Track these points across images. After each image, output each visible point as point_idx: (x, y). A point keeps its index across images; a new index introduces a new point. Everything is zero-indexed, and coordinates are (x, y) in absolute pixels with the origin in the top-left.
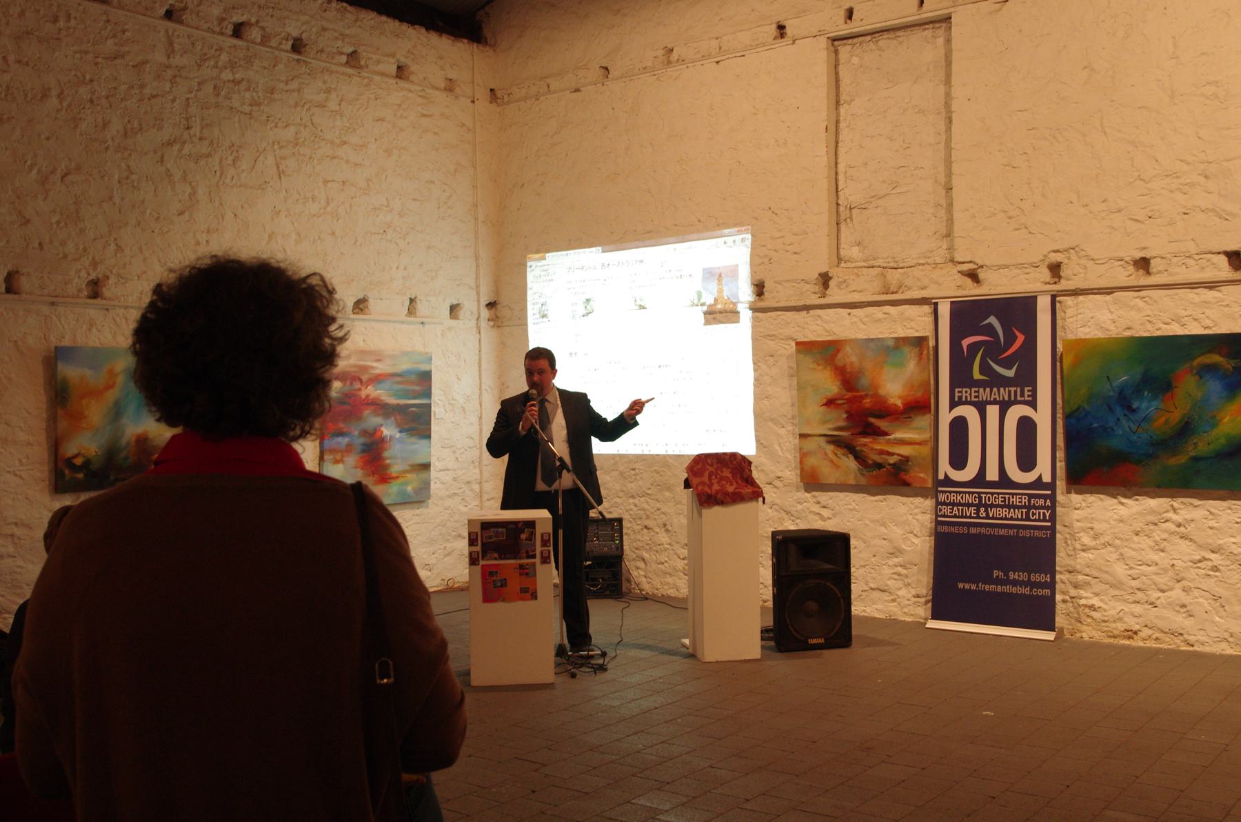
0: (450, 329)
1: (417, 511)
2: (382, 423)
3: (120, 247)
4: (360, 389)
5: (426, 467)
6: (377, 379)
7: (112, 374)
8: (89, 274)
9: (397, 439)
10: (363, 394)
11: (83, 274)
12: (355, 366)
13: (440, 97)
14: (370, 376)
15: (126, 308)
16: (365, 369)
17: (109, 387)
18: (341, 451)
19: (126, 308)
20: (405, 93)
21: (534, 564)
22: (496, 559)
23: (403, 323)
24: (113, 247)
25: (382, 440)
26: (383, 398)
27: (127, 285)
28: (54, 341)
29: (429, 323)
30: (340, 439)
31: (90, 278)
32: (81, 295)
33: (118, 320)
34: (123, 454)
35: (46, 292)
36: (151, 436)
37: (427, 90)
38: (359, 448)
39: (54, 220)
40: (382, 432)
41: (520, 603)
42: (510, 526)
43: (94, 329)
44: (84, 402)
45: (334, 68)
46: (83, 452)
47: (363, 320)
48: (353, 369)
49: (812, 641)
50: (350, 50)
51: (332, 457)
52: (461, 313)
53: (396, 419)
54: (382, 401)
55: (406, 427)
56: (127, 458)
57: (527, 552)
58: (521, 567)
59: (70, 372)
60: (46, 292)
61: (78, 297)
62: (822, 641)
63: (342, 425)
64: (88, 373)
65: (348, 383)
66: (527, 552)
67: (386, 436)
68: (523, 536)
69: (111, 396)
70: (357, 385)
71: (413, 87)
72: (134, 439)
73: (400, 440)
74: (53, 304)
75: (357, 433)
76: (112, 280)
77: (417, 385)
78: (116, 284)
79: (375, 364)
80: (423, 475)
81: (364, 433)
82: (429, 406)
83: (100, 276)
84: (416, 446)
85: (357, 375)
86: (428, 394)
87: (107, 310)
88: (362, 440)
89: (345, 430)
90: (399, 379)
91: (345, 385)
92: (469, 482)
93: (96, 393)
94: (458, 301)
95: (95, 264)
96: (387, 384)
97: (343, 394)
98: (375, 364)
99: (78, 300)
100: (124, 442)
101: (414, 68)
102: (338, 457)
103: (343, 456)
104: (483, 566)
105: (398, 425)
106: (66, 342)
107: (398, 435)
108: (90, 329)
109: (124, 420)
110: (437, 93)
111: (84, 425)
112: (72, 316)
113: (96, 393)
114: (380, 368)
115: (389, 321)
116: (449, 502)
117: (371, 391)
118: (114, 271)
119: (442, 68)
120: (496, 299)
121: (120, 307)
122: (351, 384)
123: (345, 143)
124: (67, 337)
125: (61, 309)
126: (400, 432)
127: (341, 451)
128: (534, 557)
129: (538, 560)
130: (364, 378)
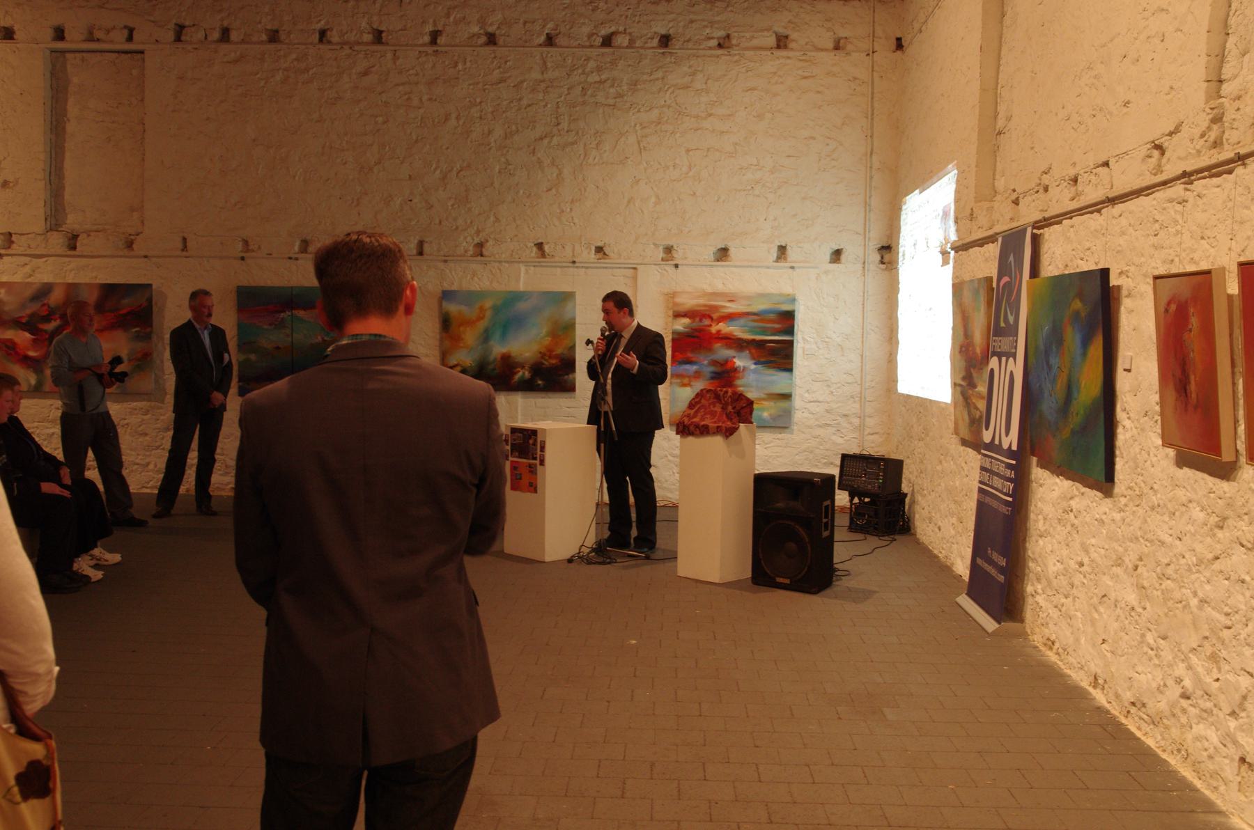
0: (826, 272)
1: (780, 436)
2: (735, 355)
3: (498, 219)
4: (711, 325)
5: (787, 397)
6: (730, 317)
7: (482, 309)
8: (473, 240)
9: (752, 370)
10: (714, 329)
11: (469, 239)
12: (705, 306)
13: (829, 58)
14: (722, 314)
15: (500, 262)
16: (716, 308)
17: (480, 318)
18: (689, 377)
19: (500, 262)
20: (782, 61)
21: (536, 465)
22: (517, 457)
23: (768, 268)
24: (492, 219)
25: (735, 370)
26: (735, 334)
27: (502, 246)
28: (447, 287)
29: (799, 268)
30: (687, 367)
31: (476, 242)
32: (466, 255)
33: (494, 271)
34: (491, 367)
35: (442, 253)
36: (513, 355)
37: (809, 53)
38: (708, 375)
39: (450, 204)
40: (734, 363)
41: (529, 494)
42: (525, 433)
43: (476, 278)
44: (462, 329)
45: (702, 52)
46: (461, 363)
47: (727, 266)
48: (702, 308)
49: (779, 580)
50: (722, 33)
51: (679, 381)
52: (843, 257)
53: (750, 352)
54: (734, 336)
55: (762, 360)
56: (494, 369)
57: (533, 455)
58: (530, 466)
59: (453, 308)
60: (442, 253)
61: (464, 256)
62: (787, 581)
63: (690, 355)
64: (463, 308)
65: (697, 319)
66: (533, 455)
67: (739, 367)
68: (531, 442)
69: (482, 325)
70: (706, 322)
71: (791, 54)
72: (499, 356)
73: (755, 371)
74: (446, 261)
75: (706, 362)
76: (491, 242)
77: (778, 323)
78: (494, 245)
79: (728, 304)
80: (783, 404)
81: (714, 363)
82: (791, 343)
83: (482, 240)
84: (774, 378)
85: (707, 313)
86: (790, 330)
87: (486, 264)
88: (712, 369)
89: (693, 359)
90: (756, 318)
91: (692, 323)
92: (845, 416)
93: (470, 323)
94: (839, 245)
95: (478, 232)
96: (742, 321)
97: (692, 329)
98: (728, 304)
99: (465, 258)
100: (491, 358)
101: (794, 35)
102: (686, 381)
103: (690, 381)
104: (512, 462)
105: (753, 358)
106: (454, 288)
107: (753, 367)
108: (472, 278)
109: (492, 343)
110: (823, 54)
111: (462, 345)
112: (460, 269)
113: (470, 323)
114: (733, 308)
115: (751, 267)
116: (820, 432)
117: (724, 328)
118: (492, 237)
119: (829, 30)
120: (889, 243)
121: (495, 261)
122: (701, 320)
123: (710, 115)
124: (455, 284)
125: (452, 265)
126: (755, 364)
127: (689, 377)
128: (535, 459)
129: (537, 462)
130: (715, 316)
